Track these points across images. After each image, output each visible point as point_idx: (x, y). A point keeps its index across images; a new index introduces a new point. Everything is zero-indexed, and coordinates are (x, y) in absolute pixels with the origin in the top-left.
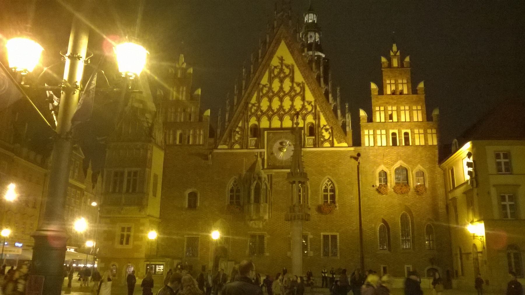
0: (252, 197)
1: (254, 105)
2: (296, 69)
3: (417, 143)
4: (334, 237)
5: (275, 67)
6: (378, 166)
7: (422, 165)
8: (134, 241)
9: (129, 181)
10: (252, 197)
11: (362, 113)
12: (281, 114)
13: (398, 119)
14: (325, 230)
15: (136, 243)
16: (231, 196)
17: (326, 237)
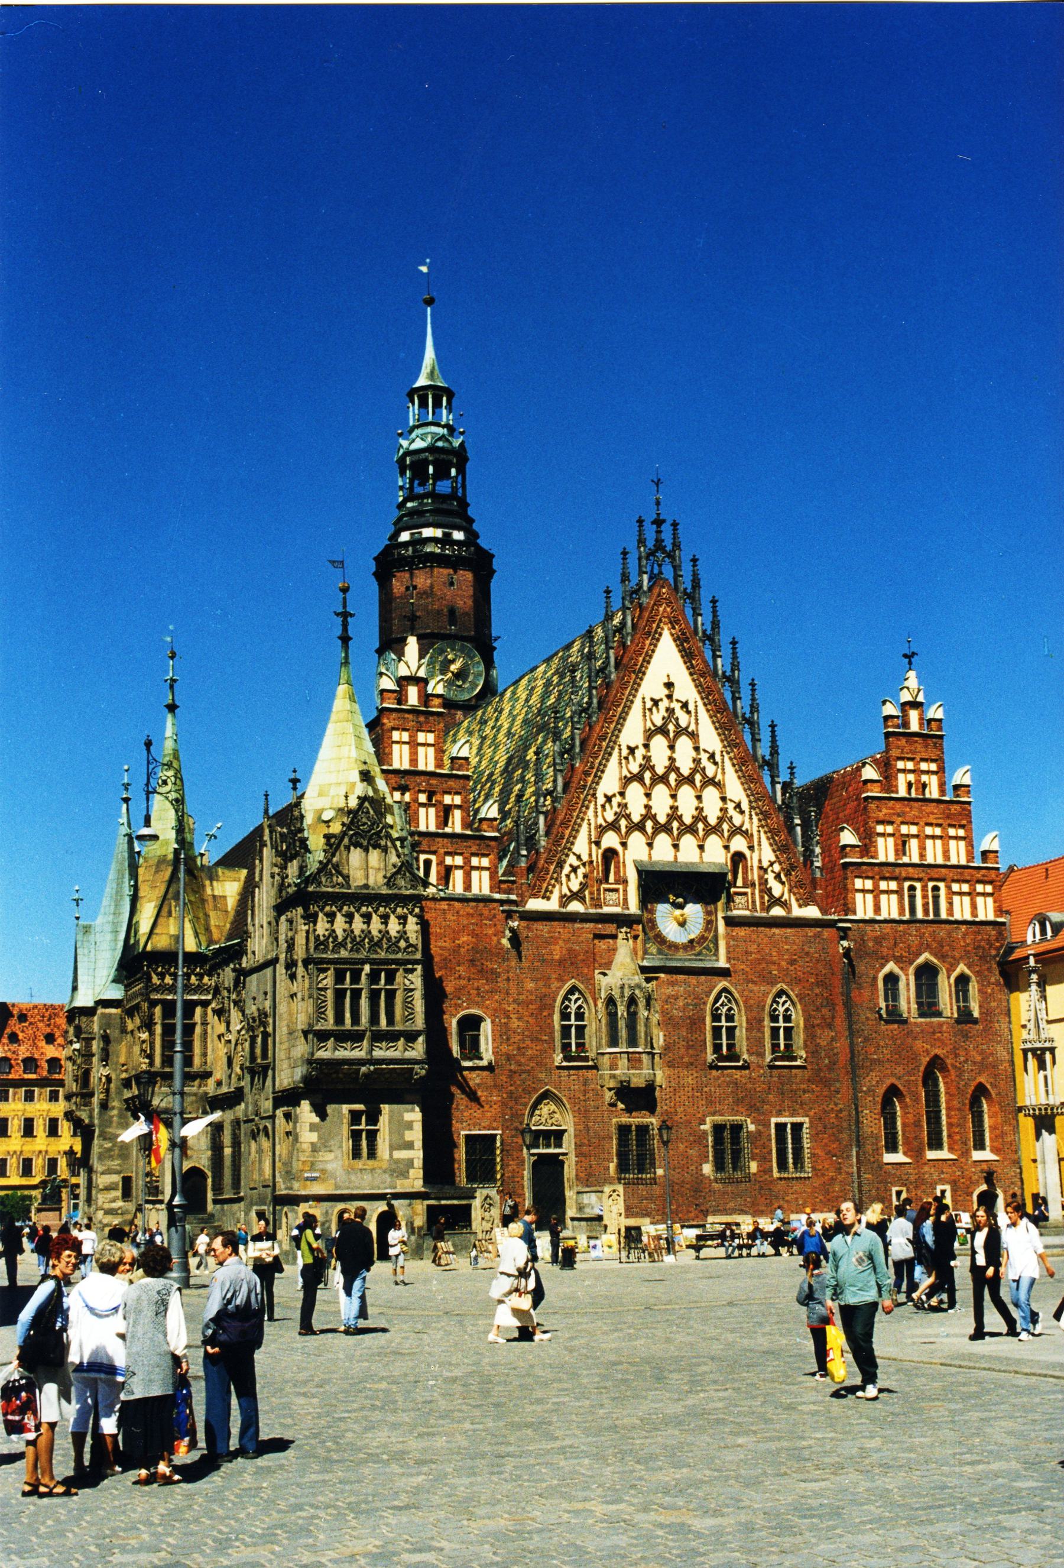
0: (623, 1033)
1: (609, 799)
2: (702, 709)
3: (957, 916)
4: (797, 1127)
5: (656, 702)
6: (883, 966)
7: (969, 968)
8: (392, 1148)
9: (374, 996)
10: (623, 1033)
11: (848, 837)
12: (672, 826)
13: (922, 856)
14: (779, 1114)
16: (563, 1027)
17: (781, 1127)
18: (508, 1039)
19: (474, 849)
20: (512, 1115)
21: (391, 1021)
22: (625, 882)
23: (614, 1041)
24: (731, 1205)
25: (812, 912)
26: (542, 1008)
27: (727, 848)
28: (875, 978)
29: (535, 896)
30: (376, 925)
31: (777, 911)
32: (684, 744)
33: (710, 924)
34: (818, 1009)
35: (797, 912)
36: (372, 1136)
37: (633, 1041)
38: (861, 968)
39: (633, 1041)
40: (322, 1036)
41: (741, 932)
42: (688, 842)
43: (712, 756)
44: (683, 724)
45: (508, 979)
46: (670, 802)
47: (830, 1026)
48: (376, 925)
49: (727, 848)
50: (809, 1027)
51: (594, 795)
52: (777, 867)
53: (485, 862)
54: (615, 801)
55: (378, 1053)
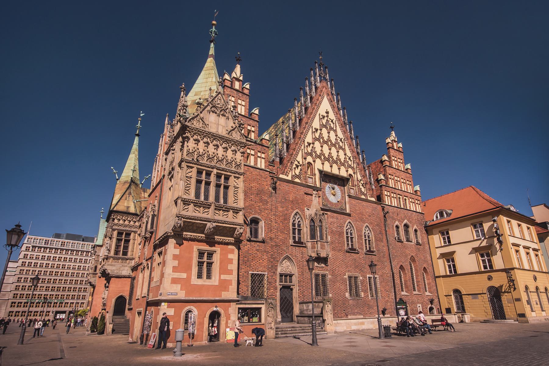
1: (309, 144)
5: (324, 117)
6: (395, 222)
8: (220, 274)
13: (401, 188)
15: (223, 277)
18: (271, 230)
19: (259, 149)
20: (272, 266)
21: (226, 201)
22: (315, 175)
23: (313, 236)
24: (356, 311)
25: (373, 199)
26: (285, 219)
27: (347, 171)
28: (393, 226)
29: (282, 174)
30: (220, 151)
31: (363, 197)
32: (332, 133)
33: (343, 197)
34: (378, 235)
35: (369, 198)
36: (210, 265)
37: (322, 238)
38: (389, 221)
39: (322, 238)
40: (186, 202)
41: (354, 201)
42: (335, 166)
43: (341, 140)
44: (332, 125)
45: (272, 205)
46: (329, 151)
47: (382, 241)
48: (220, 151)
49: (347, 171)
50: (376, 240)
51: (304, 141)
52: (362, 182)
53: (263, 156)
54: (311, 145)
55: (217, 217)
